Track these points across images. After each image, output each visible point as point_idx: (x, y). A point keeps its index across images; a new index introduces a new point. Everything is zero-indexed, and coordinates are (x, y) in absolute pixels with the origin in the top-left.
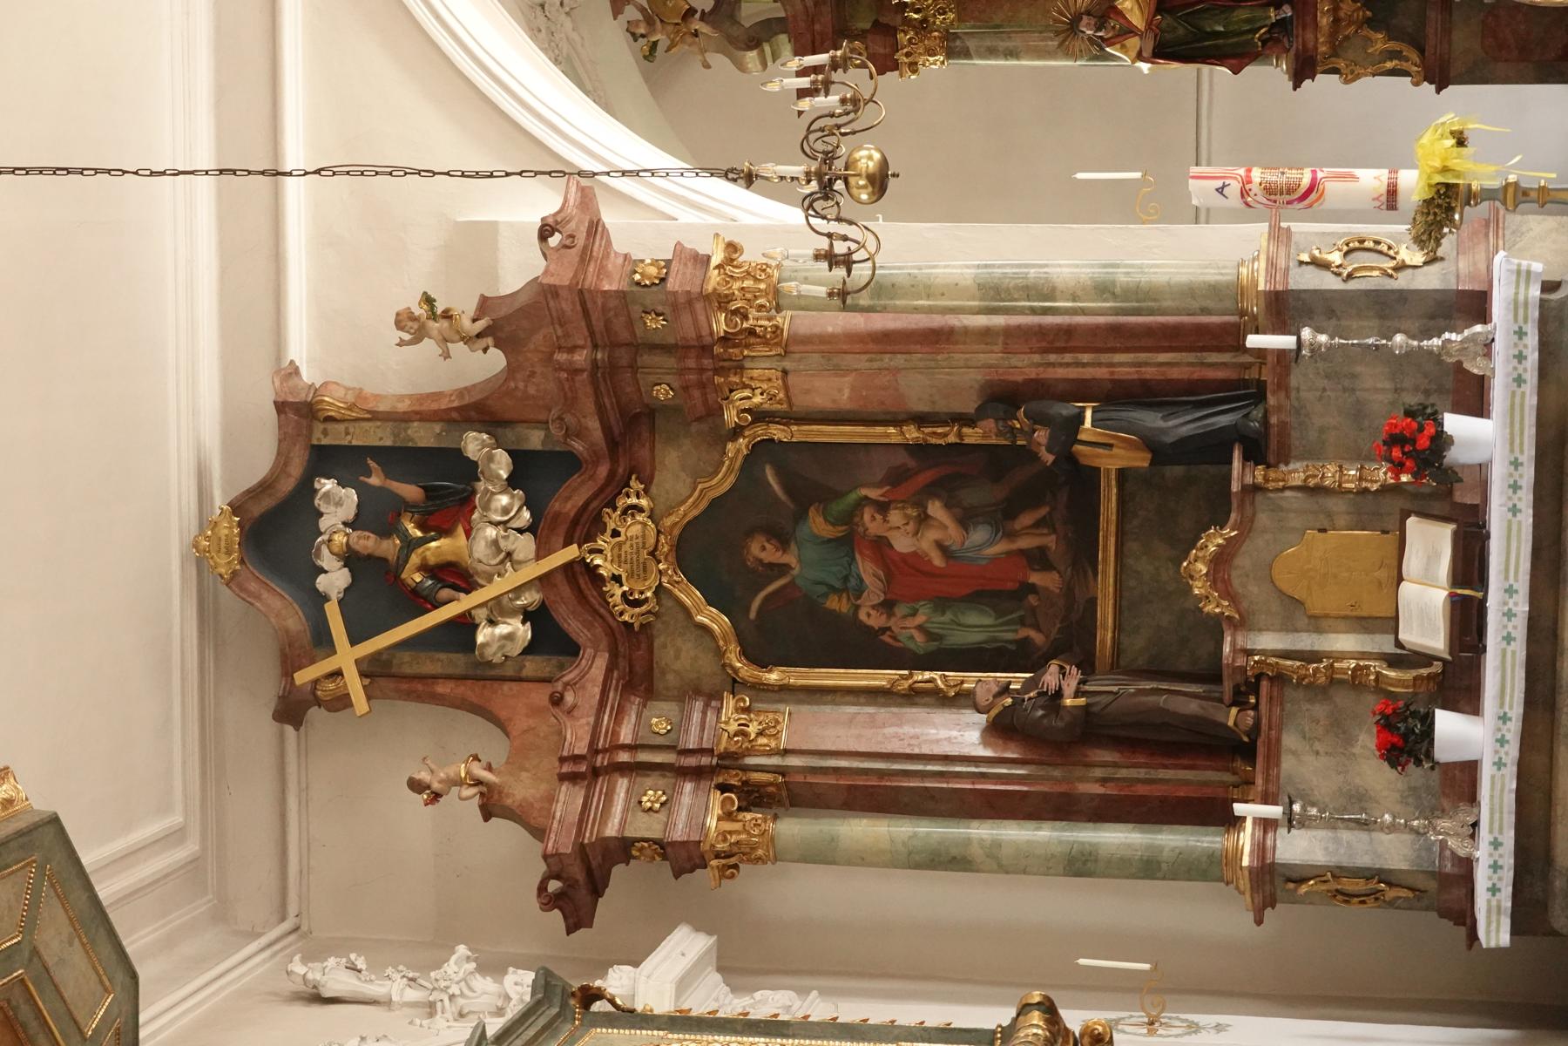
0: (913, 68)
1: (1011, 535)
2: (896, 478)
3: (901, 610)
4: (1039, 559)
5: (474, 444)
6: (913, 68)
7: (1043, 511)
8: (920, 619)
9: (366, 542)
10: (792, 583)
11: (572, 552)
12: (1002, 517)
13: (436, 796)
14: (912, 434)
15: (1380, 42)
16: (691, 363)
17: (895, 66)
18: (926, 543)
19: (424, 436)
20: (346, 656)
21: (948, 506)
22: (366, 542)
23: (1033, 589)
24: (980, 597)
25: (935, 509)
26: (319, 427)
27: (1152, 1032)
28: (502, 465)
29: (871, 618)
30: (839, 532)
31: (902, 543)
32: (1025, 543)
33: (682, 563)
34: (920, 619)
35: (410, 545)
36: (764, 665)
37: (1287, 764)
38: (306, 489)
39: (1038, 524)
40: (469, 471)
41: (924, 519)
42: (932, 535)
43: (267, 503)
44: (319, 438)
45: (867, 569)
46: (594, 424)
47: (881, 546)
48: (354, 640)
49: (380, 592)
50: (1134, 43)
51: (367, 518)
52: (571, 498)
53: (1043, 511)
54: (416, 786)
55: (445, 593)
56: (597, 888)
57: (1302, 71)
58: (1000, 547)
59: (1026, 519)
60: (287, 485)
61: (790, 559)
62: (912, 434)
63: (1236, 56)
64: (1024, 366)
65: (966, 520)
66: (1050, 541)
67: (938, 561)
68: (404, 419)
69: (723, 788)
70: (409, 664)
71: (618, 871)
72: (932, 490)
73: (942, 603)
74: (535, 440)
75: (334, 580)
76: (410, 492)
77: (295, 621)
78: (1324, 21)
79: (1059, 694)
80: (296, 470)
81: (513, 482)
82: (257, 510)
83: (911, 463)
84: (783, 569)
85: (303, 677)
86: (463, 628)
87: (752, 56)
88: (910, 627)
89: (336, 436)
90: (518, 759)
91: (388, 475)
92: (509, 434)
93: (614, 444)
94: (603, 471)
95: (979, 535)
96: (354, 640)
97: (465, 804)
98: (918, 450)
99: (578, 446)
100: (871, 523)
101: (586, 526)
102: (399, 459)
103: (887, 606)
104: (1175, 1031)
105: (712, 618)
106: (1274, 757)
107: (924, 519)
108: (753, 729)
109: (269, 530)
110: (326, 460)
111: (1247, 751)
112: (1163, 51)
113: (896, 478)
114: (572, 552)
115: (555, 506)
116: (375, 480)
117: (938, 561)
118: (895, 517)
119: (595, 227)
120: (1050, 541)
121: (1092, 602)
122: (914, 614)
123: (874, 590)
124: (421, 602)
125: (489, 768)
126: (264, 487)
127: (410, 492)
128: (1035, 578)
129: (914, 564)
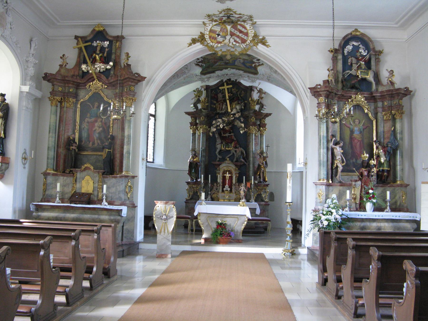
0: (191, 128)
1: (97, 140)
2: (105, 124)
3: (87, 124)
4: (94, 144)
5: (111, 64)
6: (191, 128)
7: (100, 144)
8: (86, 127)
9: (98, 49)
10: (91, 109)
11: (95, 77)
12: (100, 138)
13: (61, 58)
14: (111, 125)
15: (191, 193)
16: (120, 94)
17: (191, 126)
18: (96, 128)
19: (113, 57)
20: (82, 45)
21: (101, 131)
22: (98, 49)
23: (89, 143)
24: (89, 135)
25: (101, 129)
26: (115, 42)
27: (23, 158)
28: (108, 67)
29: (87, 120)
30: (98, 115)
31: (96, 124)
32: (96, 142)
33: (95, 93)
34: (86, 127)
35: (98, 54)
36: (80, 105)
37: (62, 177)
38: (107, 40)
39: (98, 143)
40: (108, 63)
41: (99, 127)
42: (97, 128)
43: (105, 34)
44: (114, 41)
45: (93, 119)
46: (112, 81)
47: (96, 121)
48: (85, 47)
49: (91, 50)
50: (192, 160)
51: (102, 49)
52: (103, 77)
53: (100, 144)
54: (64, 55)
55: (91, 60)
56: (49, 81)
57: (188, 183)
58: (95, 138)
59: (99, 142)
60: (107, 37)
61: (95, 108)
62: (111, 125)
63: (190, 173)
64: (118, 142)
65: (99, 133)
66: (96, 145)
67: (94, 129)
68: (115, 54)
69: (61, 99)
70: (82, 54)
71: (51, 84)
72: (104, 129)
73: (88, 130)
74: (112, 72)
75: (95, 44)
76: (105, 55)
77: (88, 38)
78: (194, 186)
79: (72, 146)
80: (110, 38)
81: (106, 69)
82: (104, 33)
83: (107, 126)
84: (93, 107)
85: (80, 39)
86: (85, 62)
87: (192, 105)
88: (85, 125)
89: (114, 44)
90: (68, 70)
91: (107, 51)
92: (113, 69)
93: (111, 83)
94: (107, 82)
95: (97, 135)
96: (85, 47)
97: (60, 62)
98: (109, 127)
99: (110, 78)
100: (99, 120)
101: (99, 79)
102: (110, 54)
103: (88, 122)
104: (24, 162)
105: (87, 97)
106: (62, 175)
107: (99, 127)
108: (70, 103)
109: (100, 34)
110: (111, 42)
111: (64, 172)
112: (191, 164)
113: (105, 124)
114: (95, 77)
115: (102, 75)
116: (107, 50)
117: (94, 129)
118: (100, 123)
119: (139, 81)
120: (96, 145)
121: (87, 151)
122: (87, 126)
123: (90, 120)
124: (90, 56)
125: (66, 66)
126: (107, 34)
127: (105, 55)
128: (91, 143)
129: (93, 126)
